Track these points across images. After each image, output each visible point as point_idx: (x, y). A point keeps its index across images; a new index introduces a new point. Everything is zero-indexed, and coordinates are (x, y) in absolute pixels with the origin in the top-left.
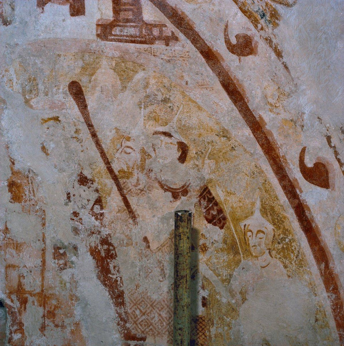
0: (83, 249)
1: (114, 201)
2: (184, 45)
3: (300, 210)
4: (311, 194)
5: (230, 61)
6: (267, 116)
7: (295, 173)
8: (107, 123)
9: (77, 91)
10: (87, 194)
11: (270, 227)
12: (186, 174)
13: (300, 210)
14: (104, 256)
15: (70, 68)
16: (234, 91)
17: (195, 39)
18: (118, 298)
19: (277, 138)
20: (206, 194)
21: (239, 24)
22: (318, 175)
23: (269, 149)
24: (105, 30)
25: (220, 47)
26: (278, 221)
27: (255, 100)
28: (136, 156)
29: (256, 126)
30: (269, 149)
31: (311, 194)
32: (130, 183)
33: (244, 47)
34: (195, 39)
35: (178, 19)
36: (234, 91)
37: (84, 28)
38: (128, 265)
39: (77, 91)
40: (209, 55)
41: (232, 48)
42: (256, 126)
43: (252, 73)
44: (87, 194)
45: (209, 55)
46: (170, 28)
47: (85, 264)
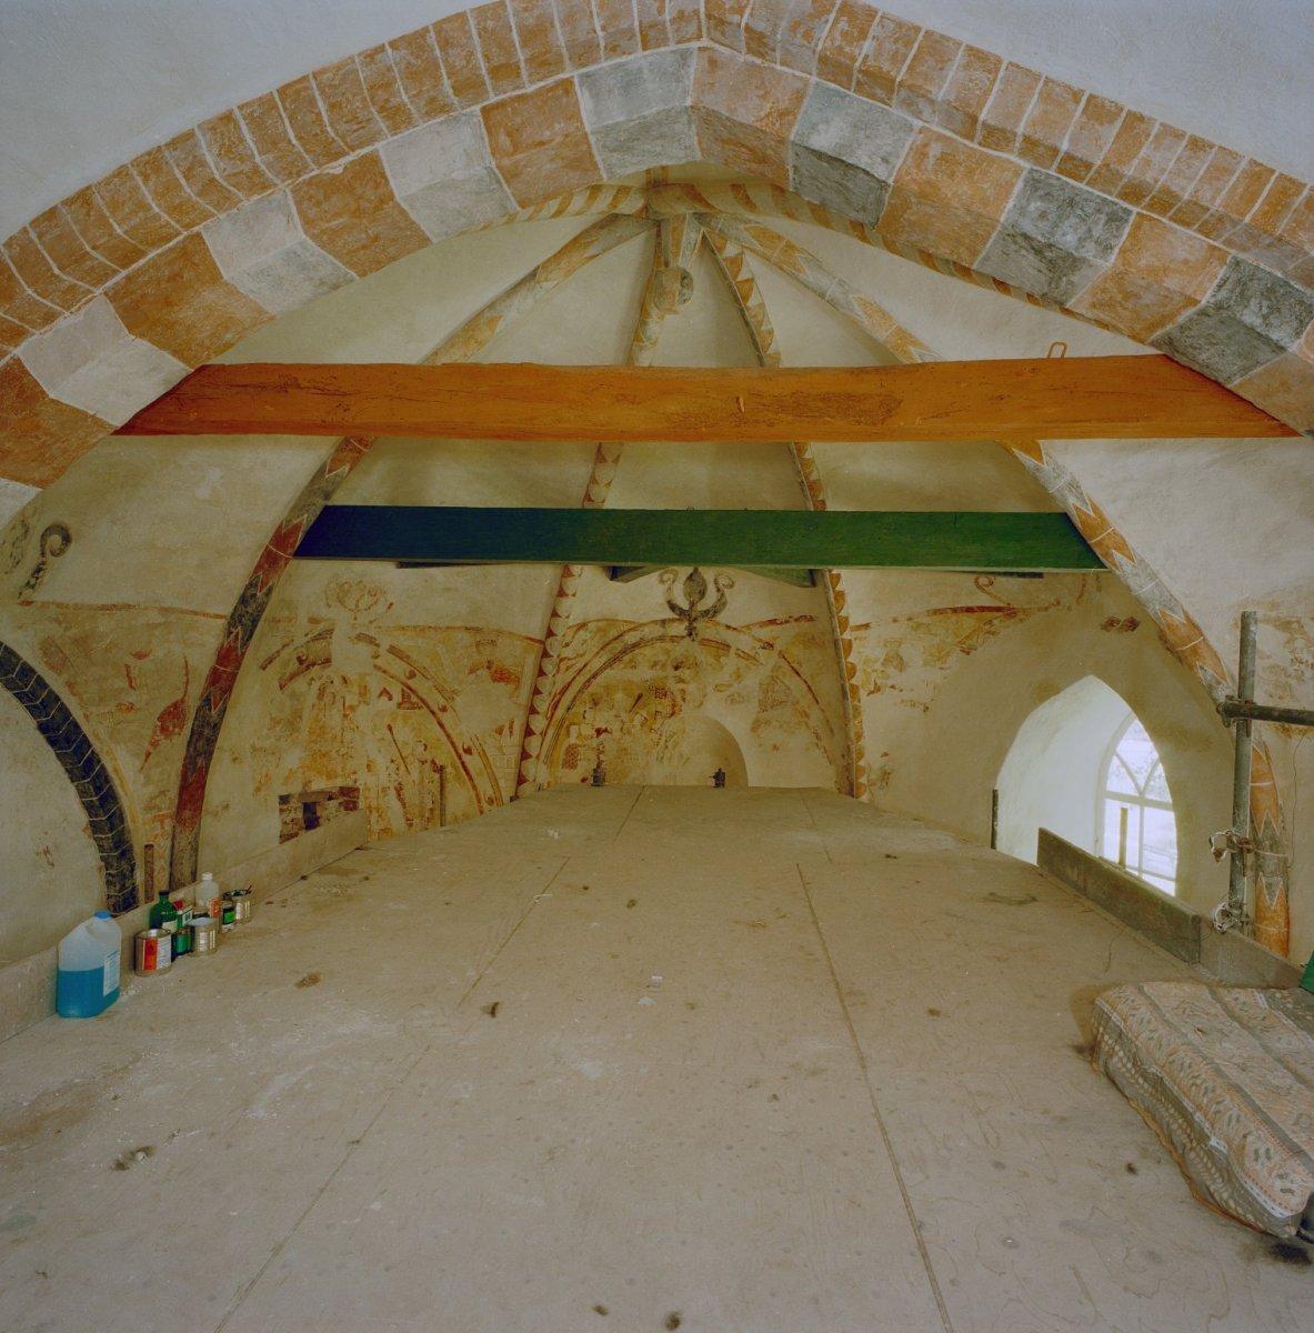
0: (392, 788)
1: (403, 768)
2: (425, 710)
3: (463, 763)
4: (466, 758)
5: (439, 714)
6: (450, 732)
7: (461, 751)
8: (400, 738)
9: (390, 728)
10: (393, 766)
11: (453, 771)
12: (428, 756)
13: (463, 763)
14: (399, 790)
15: (387, 721)
16: (441, 725)
17: (428, 707)
18: (404, 805)
19: (455, 740)
20: (433, 762)
21: (442, 702)
22: (468, 751)
23: (453, 744)
24: (399, 705)
25: (436, 709)
26: (456, 769)
27: (447, 726)
28: (410, 751)
29: (448, 736)
30: (453, 744)
31: (466, 758)
32: (408, 761)
33: (444, 709)
34: (428, 707)
35: (423, 701)
36: (441, 725)
37: (392, 705)
38: (406, 794)
39: (390, 728)
40: (433, 712)
41: (440, 710)
42: (448, 736)
43: (446, 718)
44: (393, 766)
45: (433, 712)
46: (421, 704)
47: (392, 793)
